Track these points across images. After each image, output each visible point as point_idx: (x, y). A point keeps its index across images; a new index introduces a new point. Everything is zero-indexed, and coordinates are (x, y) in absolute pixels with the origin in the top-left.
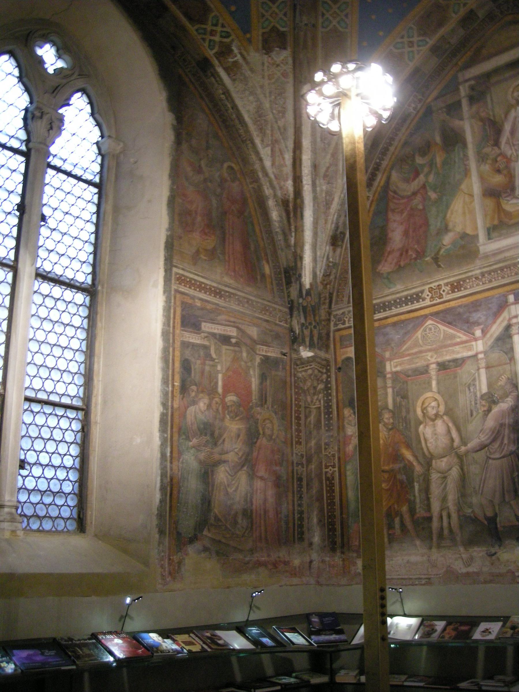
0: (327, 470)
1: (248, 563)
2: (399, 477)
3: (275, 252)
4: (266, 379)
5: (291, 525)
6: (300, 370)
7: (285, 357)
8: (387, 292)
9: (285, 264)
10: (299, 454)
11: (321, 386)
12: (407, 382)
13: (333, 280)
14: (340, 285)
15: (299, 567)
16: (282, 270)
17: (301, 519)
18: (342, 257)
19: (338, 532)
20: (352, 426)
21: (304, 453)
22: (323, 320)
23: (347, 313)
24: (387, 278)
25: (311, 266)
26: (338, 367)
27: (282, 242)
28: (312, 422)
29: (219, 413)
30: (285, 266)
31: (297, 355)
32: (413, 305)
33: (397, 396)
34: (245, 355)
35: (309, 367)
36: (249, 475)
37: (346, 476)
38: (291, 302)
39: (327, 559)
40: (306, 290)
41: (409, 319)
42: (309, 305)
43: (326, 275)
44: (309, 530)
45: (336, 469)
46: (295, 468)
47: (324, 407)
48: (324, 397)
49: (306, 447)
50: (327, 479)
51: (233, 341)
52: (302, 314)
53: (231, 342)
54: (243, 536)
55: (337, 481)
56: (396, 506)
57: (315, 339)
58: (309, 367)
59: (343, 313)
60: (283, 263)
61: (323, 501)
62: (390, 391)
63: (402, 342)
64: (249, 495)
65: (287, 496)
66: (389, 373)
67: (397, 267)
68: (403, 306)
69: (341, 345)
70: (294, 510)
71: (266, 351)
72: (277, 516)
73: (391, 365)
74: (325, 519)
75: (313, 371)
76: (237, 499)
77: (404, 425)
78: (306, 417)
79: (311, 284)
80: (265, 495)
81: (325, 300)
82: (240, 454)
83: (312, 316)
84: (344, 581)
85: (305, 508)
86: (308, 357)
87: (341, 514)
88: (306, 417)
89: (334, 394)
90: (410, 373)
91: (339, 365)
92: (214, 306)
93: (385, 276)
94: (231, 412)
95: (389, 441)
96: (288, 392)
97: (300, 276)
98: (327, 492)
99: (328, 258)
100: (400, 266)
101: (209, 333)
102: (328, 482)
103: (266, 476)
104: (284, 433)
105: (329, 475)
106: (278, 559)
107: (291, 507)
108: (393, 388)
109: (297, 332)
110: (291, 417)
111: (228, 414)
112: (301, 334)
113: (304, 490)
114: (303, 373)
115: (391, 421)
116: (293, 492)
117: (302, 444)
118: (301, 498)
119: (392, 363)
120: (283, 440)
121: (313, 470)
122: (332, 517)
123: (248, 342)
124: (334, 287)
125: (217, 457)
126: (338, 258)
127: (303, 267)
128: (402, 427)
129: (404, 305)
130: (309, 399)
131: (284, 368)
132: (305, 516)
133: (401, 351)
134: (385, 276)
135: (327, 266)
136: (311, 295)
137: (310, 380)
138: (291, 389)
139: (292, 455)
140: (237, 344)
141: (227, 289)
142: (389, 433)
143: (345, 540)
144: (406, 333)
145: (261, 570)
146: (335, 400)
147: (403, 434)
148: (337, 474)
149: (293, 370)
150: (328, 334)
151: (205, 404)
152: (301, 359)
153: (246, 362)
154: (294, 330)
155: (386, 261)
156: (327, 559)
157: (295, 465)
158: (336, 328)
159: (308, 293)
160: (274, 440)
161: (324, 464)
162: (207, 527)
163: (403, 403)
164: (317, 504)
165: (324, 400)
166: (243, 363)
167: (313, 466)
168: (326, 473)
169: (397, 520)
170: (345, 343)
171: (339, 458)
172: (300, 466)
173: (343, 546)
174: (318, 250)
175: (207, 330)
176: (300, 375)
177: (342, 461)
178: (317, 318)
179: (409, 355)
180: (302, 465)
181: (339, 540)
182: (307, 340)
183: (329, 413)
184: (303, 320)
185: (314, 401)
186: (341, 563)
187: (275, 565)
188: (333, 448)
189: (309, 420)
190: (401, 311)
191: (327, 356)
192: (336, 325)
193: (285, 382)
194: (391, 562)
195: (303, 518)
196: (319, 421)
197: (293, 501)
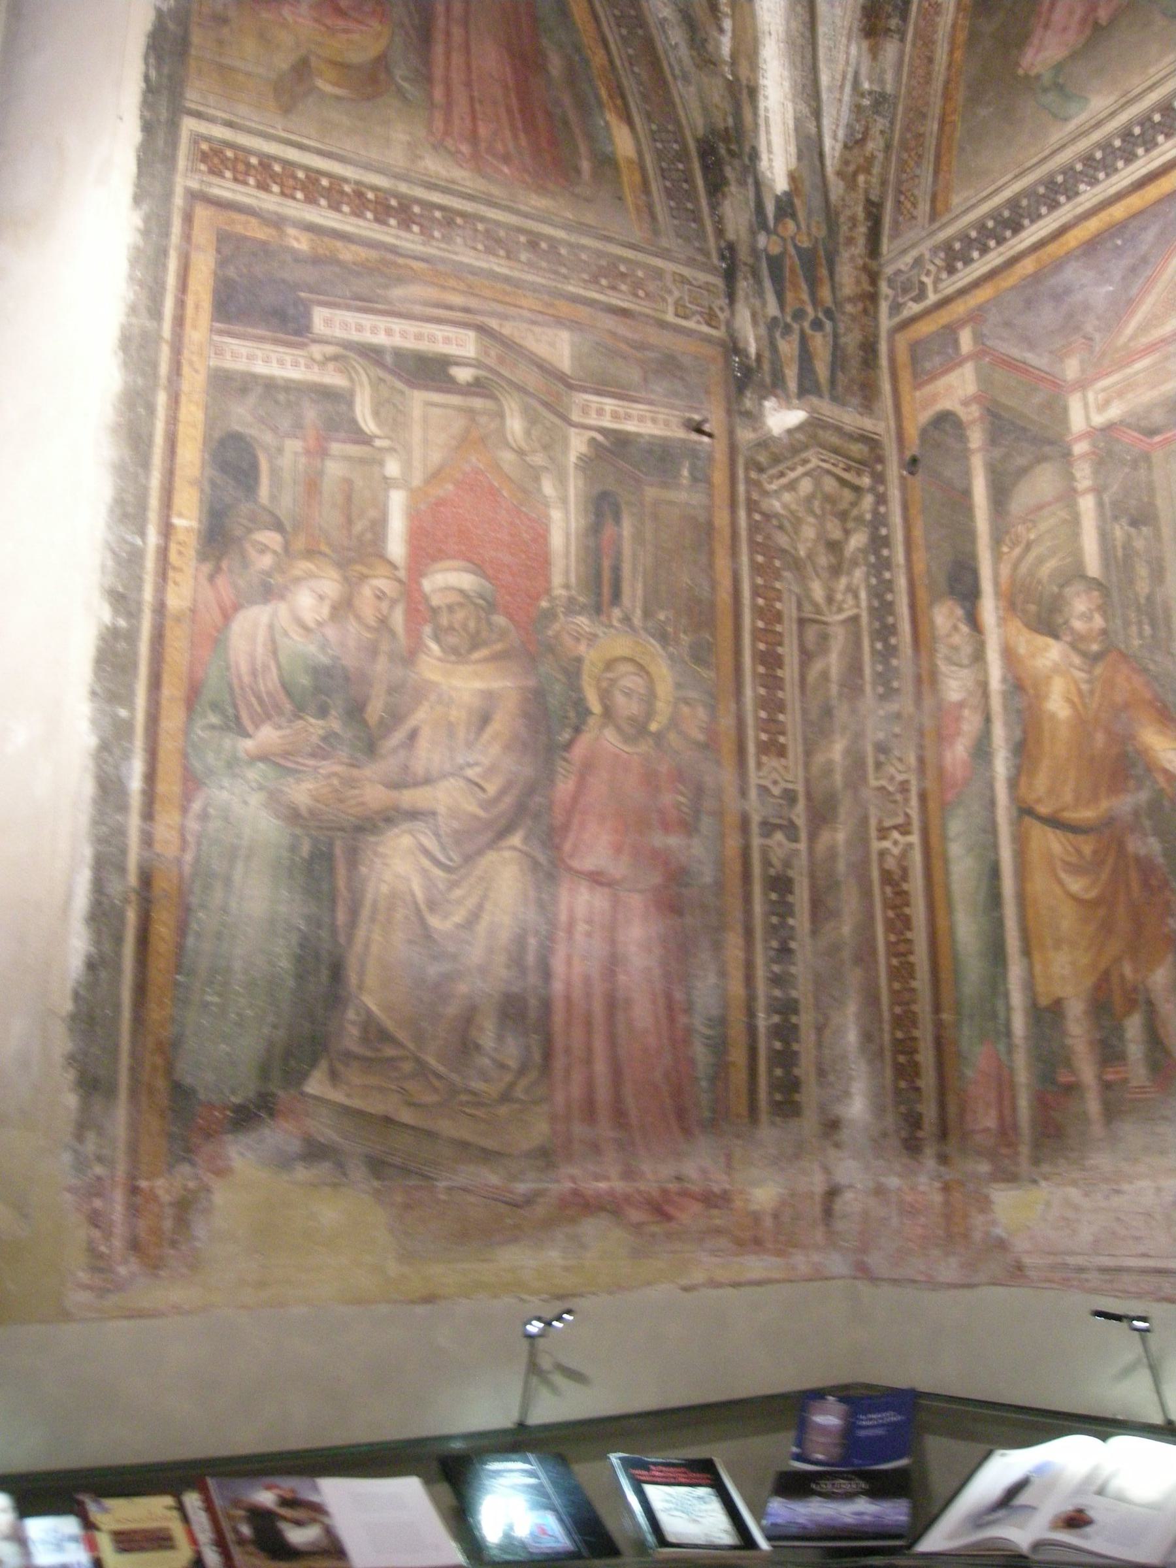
0: (886, 844)
1: (529, 1200)
2: (1135, 845)
3: (659, 80)
4: (617, 519)
5: (738, 1055)
6: (773, 487)
7: (706, 439)
8: (1057, 135)
9: (700, 122)
10: (776, 791)
11: (857, 540)
12: (1147, 458)
13: (880, 156)
14: (902, 166)
15: (776, 1216)
16: (692, 145)
17: (786, 1032)
18: (906, 69)
19: (928, 1081)
20: (961, 666)
21: (800, 788)
22: (850, 300)
23: (927, 256)
24: (1059, 88)
25: (790, 115)
26: (908, 455)
27: (684, 52)
28: (834, 673)
29: (392, 633)
30: (701, 132)
31: (755, 430)
32: (1155, 153)
33: (1116, 518)
34: (515, 425)
35: (800, 470)
36: (535, 865)
37: (945, 860)
38: (729, 252)
39: (893, 1182)
40: (778, 199)
41: (1141, 212)
42: (792, 251)
43: (854, 142)
44: (821, 1073)
45: (915, 839)
46: (756, 841)
47: (872, 610)
48: (867, 576)
49: (807, 766)
50: (887, 878)
51: (463, 375)
52: (768, 284)
53: (452, 380)
54: (506, 1097)
55: (916, 885)
56: (1127, 969)
57: (822, 370)
58: (800, 470)
59: (918, 262)
60: (694, 122)
61: (876, 962)
62: (1087, 505)
63: (1123, 306)
64: (532, 941)
65: (717, 947)
66: (1081, 437)
67: (1088, 32)
68: (1116, 170)
69: (915, 375)
70: (751, 998)
71: (615, 416)
72: (672, 1019)
73: (1086, 406)
74: (881, 1030)
75: (818, 484)
76: (475, 954)
77: (1147, 630)
78: (806, 657)
79: (792, 177)
80: (613, 942)
81: (854, 226)
82: (492, 789)
83: (804, 286)
84: (949, 1269)
85: (802, 991)
86: (790, 432)
87: (937, 1008)
88: (806, 657)
89: (900, 557)
90: (1158, 418)
91: (913, 448)
92: (373, 254)
93: (1047, 78)
94: (451, 628)
95: (1095, 706)
96: (722, 563)
97: (754, 155)
98: (890, 926)
99: (856, 83)
100: (1097, 27)
101: (348, 345)
102: (888, 890)
103: (618, 869)
104: (702, 713)
105: (891, 864)
106: (673, 1187)
107: (736, 988)
108: (1098, 490)
109: (752, 350)
110: (738, 652)
111: (437, 639)
112: (767, 354)
113: (801, 921)
114: (787, 497)
115: (1098, 622)
116: (748, 932)
117: (791, 754)
118: (785, 952)
119: (1091, 396)
120: (701, 737)
121: (841, 849)
122: (905, 1020)
123: (532, 379)
124: (884, 183)
125: (374, 795)
126: (889, 77)
127: (761, 121)
128: (1136, 642)
129: (1120, 164)
130: (818, 591)
131: (701, 478)
132: (805, 1020)
133: (1121, 341)
134: (1047, 78)
135: (858, 109)
136: (793, 216)
137: (811, 520)
138: (734, 553)
139: (743, 793)
140: (478, 387)
141: (436, 198)
142: (1089, 672)
143: (952, 1110)
144: (1133, 270)
145: (591, 1227)
146: (902, 582)
147: (1146, 670)
148: (917, 857)
149: (741, 488)
150: (869, 348)
151: (321, 598)
152: (765, 443)
153: (521, 453)
154: (741, 345)
155: (1046, 26)
156: (893, 1182)
157: (755, 828)
158: (897, 320)
159: (786, 207)
160: (659, 737)
161: (873, 823)
162: (324, 1064)
163: (1139, 544)
164: (854, 977)
165: (869, 587)
166: (507, 458)
167: (840, 835)
168: (882, 854)
169: (1134, 1026)
170: (928, 365)
171: (923, 797)
172: (779, 836)
173: (943, 1134)
174: (822, 66)
175: (339, 333)
176: (776, 505)
177: (932, 805)
178: (825, 293)
179: (1150, 349)
180: (791, 830)
181: (929, 1111)
182: (791, 374)
183: (884, 631)
184: (772, 308)
185: (839, 597)
186: (938, 1198)
187: (659, 1209)
188: (900, 760)
189: (817, 667)
190: (1112, 191)
191: (868, 424)
192: (896, 308)
193: (709, 529)
194: (1116, 1201)
195: (795, 1027)
196: (854, 668)
197: (749, 965)
